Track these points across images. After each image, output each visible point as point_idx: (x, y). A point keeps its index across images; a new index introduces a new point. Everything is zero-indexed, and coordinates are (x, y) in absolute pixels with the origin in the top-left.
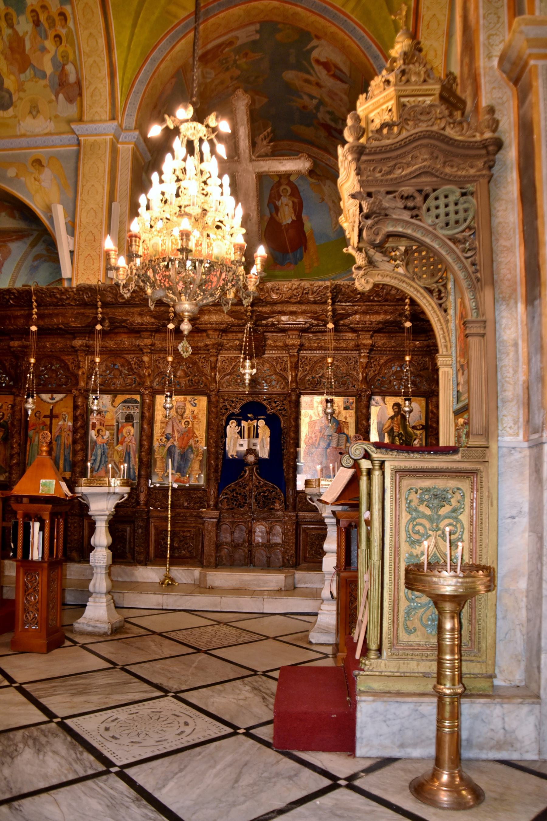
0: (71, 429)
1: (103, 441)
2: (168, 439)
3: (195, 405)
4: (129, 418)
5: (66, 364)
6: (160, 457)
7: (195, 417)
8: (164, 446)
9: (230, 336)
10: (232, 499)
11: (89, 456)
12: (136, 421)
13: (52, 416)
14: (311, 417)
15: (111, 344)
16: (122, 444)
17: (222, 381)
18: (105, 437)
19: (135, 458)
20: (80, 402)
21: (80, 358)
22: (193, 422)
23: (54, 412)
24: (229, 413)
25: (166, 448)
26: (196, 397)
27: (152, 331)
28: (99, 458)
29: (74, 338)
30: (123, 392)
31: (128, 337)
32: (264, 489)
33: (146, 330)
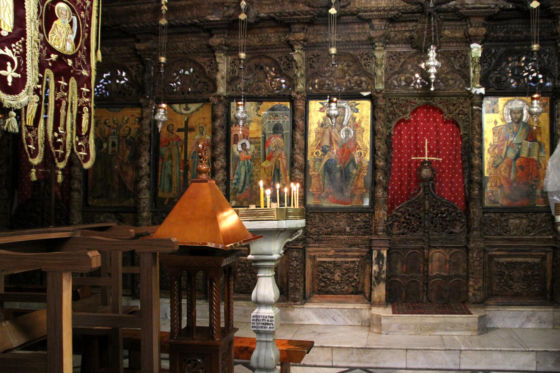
0: (210, 144)
1: (248, 156)
2: (325, 152)
3: (357, 111)
4: (277, 129)
5: (201, 67)
6: (316, 174)
7: (357, 126)
8: (321, 160)
9: (399, 27)
10: (403, 222)
11: (231, 176)
12: (287, 131)
13: (187, 129)
14: (496, 122)
15: (255, 41)
16: (269, 159)
17: (390, 81)
18: (249, 152)
19: (286, 176)
20: (220, 111)
21: (218, 60)
22: (355, 131)
23: (190, 125)
24: (398, 119)
25: (323, 163)
26: (357, 102)
27: (303, 23)
28: (242, 177)
29: (211, 36)
30: (270, 98)
31: (275, 32)
32: (443, 209)
33: (299, 22)
